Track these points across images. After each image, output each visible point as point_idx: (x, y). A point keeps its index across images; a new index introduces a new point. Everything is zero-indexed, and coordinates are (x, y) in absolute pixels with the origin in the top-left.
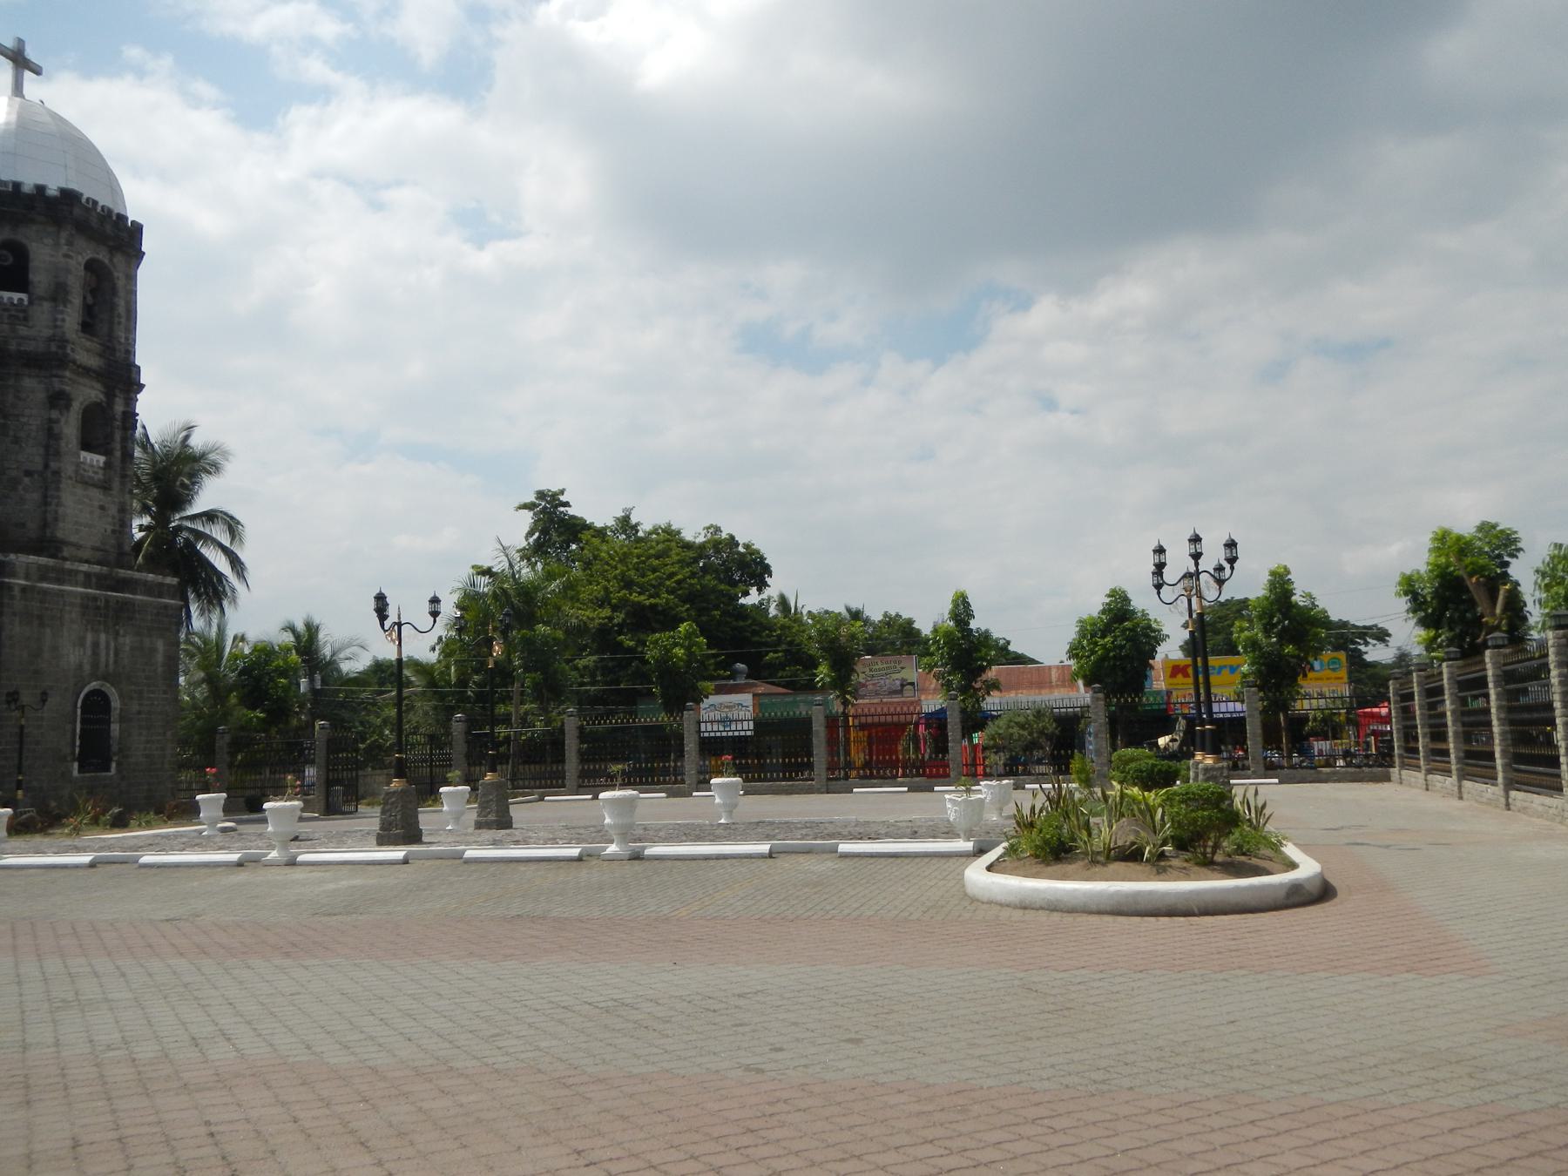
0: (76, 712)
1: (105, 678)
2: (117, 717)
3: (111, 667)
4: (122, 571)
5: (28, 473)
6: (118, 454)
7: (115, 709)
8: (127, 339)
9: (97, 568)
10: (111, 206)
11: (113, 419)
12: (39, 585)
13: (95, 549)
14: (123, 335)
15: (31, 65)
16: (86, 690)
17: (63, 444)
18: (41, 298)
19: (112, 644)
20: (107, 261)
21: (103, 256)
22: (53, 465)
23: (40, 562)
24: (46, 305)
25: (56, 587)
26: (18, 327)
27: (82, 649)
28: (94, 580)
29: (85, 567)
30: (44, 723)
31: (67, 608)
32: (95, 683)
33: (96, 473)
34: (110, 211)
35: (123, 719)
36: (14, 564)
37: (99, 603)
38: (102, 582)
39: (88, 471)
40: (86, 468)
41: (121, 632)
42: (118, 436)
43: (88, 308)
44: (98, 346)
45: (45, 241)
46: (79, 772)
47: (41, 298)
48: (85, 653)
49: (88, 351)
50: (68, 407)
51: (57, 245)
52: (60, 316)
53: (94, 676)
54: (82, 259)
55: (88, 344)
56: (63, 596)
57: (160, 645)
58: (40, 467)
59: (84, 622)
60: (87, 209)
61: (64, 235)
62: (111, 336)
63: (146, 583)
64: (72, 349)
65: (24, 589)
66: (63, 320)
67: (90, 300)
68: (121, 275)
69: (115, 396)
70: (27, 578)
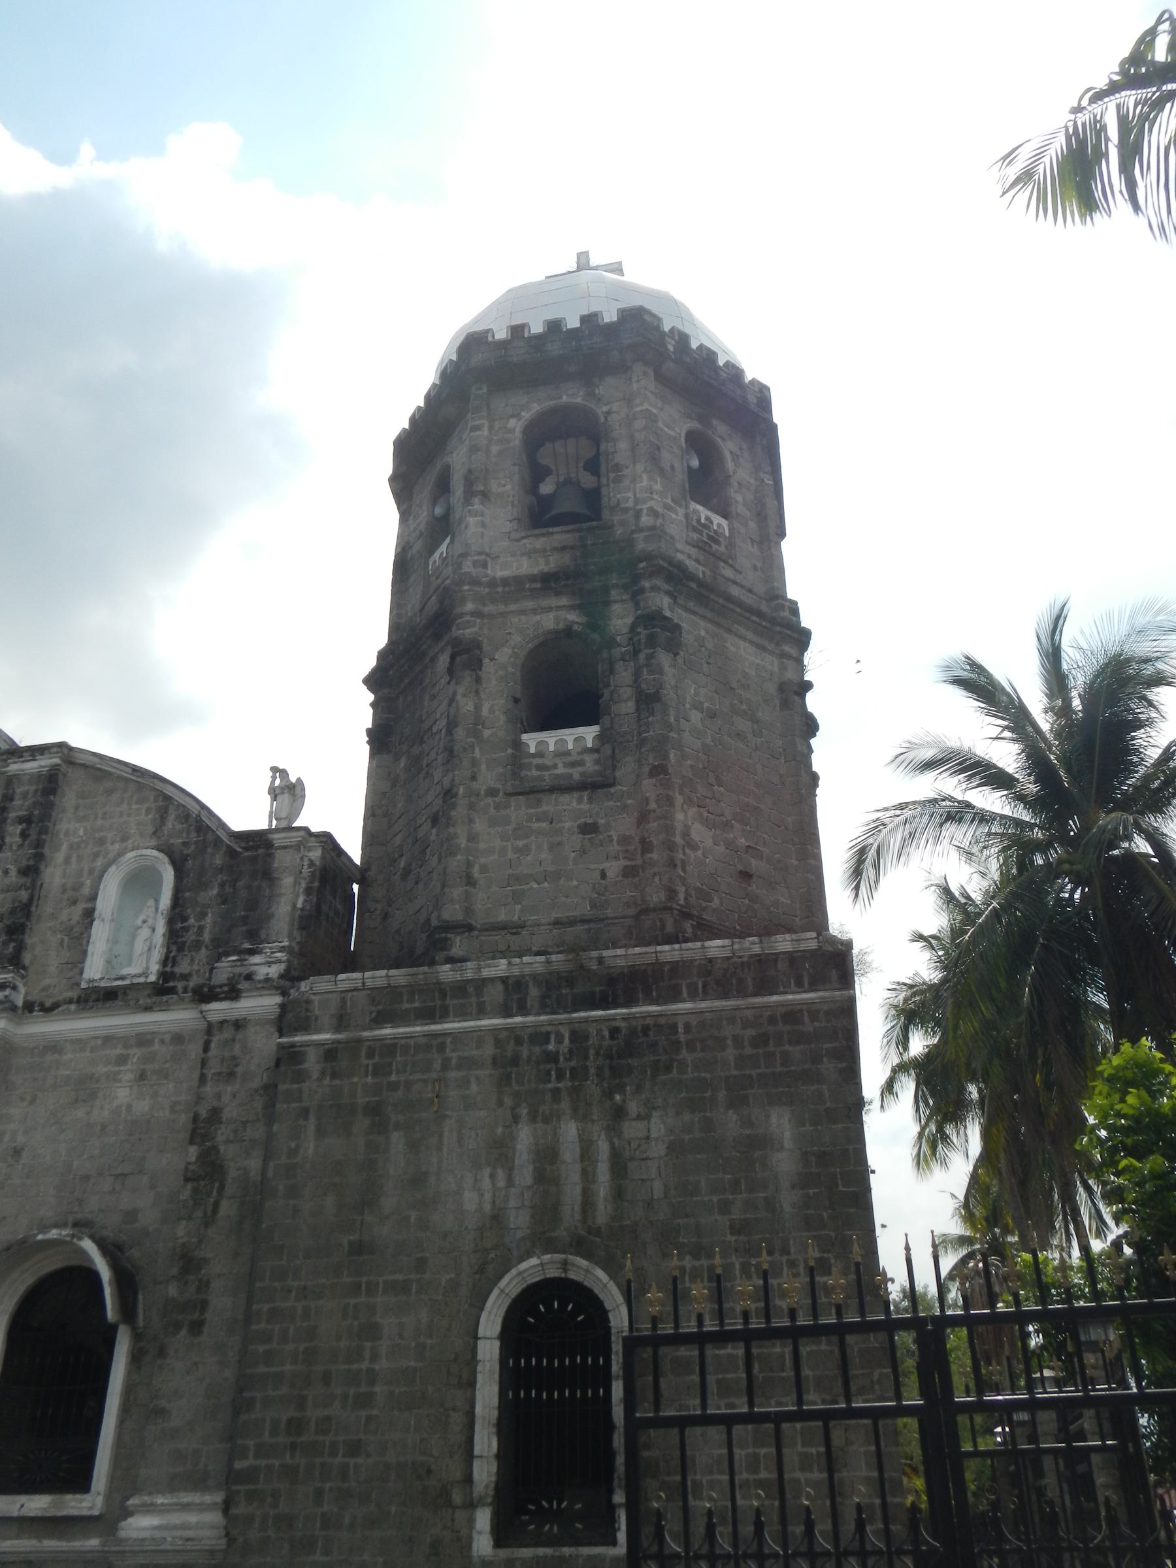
0: (472, 1361)
1: (580, 1246)
3: (603, 1213)
4: (620, 952)
11: (611, 643)
12: (366, 1034)
13: (572, 922)
16: (510, 1285)
19: (603, 1148)
23: (369, 984)
25: (418, 1029)
27: (501, 1174)
28: (534, 992)
29: (500, 967)
30: (377, 1389)
32: (534, 1261)
33: (573, 764)
36: (308, 1002)
41: (633, 1108)
42: (624, 675)
46: (498, 1543)
48: (510, 1183)
50: (475, 664)
53: (542, 1241)
54: (516, 426)
55: (539, 543)
56: (441, 1048)
59: (508, 1101)
64: (475, 564)
65: (330, 1053)
67: (588, 480)
68: (615, 407)
69: (607, 603)
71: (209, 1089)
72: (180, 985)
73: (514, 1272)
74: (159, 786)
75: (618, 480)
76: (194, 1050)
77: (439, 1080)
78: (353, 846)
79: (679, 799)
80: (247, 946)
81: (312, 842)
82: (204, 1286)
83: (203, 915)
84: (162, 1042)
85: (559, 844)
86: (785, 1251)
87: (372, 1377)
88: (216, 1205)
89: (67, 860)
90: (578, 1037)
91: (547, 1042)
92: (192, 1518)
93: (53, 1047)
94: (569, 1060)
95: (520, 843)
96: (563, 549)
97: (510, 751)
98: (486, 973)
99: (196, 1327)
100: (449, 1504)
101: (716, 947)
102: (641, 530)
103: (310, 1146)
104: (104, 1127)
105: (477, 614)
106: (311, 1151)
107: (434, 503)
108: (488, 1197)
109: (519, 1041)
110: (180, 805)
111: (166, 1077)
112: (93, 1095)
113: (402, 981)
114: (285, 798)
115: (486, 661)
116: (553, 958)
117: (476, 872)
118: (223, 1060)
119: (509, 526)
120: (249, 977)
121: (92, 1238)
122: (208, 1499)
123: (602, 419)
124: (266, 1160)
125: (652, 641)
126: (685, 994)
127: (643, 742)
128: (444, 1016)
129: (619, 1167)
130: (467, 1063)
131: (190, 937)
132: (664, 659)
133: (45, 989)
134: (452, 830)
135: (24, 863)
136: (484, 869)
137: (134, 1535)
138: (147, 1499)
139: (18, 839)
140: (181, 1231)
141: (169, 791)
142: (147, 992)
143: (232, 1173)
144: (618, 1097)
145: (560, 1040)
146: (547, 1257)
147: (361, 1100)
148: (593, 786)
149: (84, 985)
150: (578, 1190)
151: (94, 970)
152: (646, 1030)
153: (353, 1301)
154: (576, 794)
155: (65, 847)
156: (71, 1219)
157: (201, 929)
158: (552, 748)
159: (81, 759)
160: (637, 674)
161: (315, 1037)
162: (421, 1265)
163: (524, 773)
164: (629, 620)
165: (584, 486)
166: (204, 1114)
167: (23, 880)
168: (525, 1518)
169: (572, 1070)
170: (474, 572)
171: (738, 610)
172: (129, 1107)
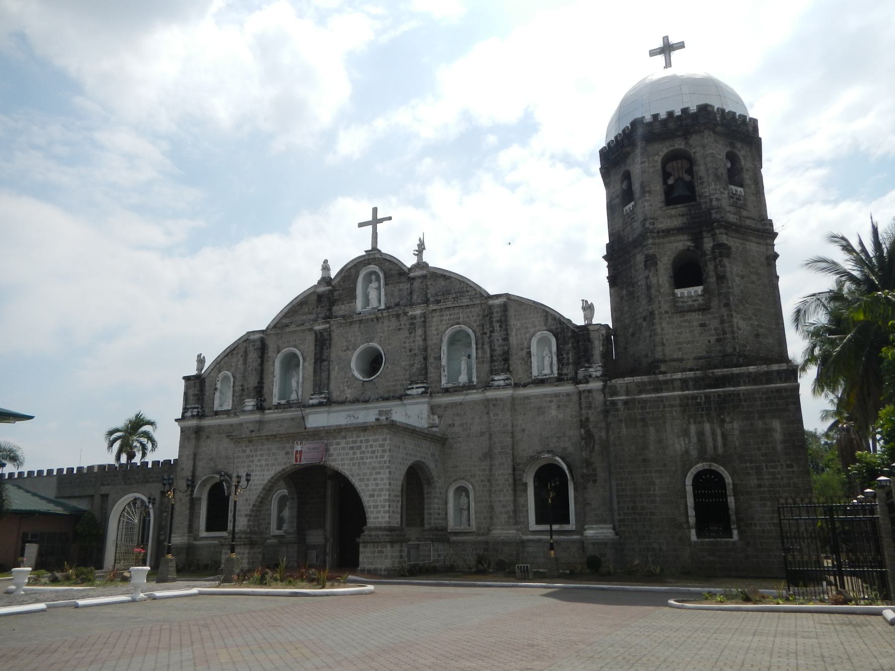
1: (714, 460)
2: (731, 490)
3: (720, 450)
4: (720, 370)
6: (713, 280)
7: (729, 484)
9: (691, 374)
11: (705, 254)
12: (637, 397)
13: (700, 358)
15: (674, 46)
16: (694, 471)
19: (719, 431)
20: (682, 147)
21: (679, 144)
23: (635, 381)
25: (654, 395)
26: (633, 224)
27: (686, 439)
28: (691, 383)
29: (679, 375)
31: (667, 409)
32: (700, 464)
33: (694, 301)
35: (736, 493)
36: (616, 386)
37: (698, 401)
38: (698, 383)
39: (688, 302)
41: (727, 419)
42: (711, 267)
44: (681, 209)
48: (690, 442)
49: (671, 217)
50: (655, 264)
53: (702, 457)
54: (659, 159)
55: (673, 212)
56: (662, 401)
57: (777, 424)
59: (686, 417)
63: (749, 375)
64: (650, 223)
65: (626, 403)
67: (687, 178)
68: (698, 149)
69: (702, 238)
70: (628, 393)
71: (584, 412)
72: (565, 377)
73: (694, 467)
74: (543, 308)
75: (702, 183)
76: (575, 398)
77: (662, 411)
78: (611, 326)
79: (734, 314)
80: (587, 365)
81: (602, 328)
82: (594, 470)
83: (568, 354)
84: (563, 396)
85: (693, 331)
86: (779, 461)
87: (655, 495)
88: (594, 447)
89: (516, 335)
90: (707, 397)
91: (697, 399)
92: (605, 531)
93: (528, 398)
94: (705, 405)
95: (679, 331)
96: (683, 215)
97: (672, 297)
98: (674, 377)
99: (595, 481)
101: (752, 369)
102: (714, 209)
103: (624, 431)
104: (550, 422)
105: (654, 244)
106: (625, 433)
107: (622, 182)
108: (683, 446)
109: (688, 399)
110: (552, 314)
111: (567, 407)
112: (544, 413)
113: (646, 380)
114: (588, 311)
115: (659, 262)
116: (697, 372)
117: (665, 341)
118: (586, 403)
119: (660, 205)
120: (590, 376)
121: (558, 456)
122: (608, 526)
123: (693, 156)
124: (607, 432)
125: (721, 255)
126: (742, 384)
127: (720, 294)
128: (661, 391)
129: (724, 437)
130: (672, 406)
131: (565, 361)
132: (726, 261)
133: (520, 379)
134: (655, 327)
135: (503, 337)
136: (667, 340)
137: (589, 535)
138: (591, 526)
140: (584, 454)
141: (547, 310)
142: (555, 379)
143: (597, 437)
144: (722, 416)
145: (701, 398)
146: (704, 463)
147: (639, 417)
148: (704, 309)
149: (533, 378)
150: (712, 444)
151: (535, 373)
152: (730, 395)
153: (645, 475)
154: (697, 313)
155: (514, 330)
156: (546, 450)
157: (568, 359)
158: (686, 295)
159: (514, 298)
160: (716, 267)
161: (620, 398)
162: (665, 465)
163: (677, 304)
164: (711, 245)
165: (686, 180)
166: (584, 419)
167: (504, 343)
168: (705, 531)
169: (706, 408)
170: (651, 227)
171: (750, 231)
172: (557, 416)
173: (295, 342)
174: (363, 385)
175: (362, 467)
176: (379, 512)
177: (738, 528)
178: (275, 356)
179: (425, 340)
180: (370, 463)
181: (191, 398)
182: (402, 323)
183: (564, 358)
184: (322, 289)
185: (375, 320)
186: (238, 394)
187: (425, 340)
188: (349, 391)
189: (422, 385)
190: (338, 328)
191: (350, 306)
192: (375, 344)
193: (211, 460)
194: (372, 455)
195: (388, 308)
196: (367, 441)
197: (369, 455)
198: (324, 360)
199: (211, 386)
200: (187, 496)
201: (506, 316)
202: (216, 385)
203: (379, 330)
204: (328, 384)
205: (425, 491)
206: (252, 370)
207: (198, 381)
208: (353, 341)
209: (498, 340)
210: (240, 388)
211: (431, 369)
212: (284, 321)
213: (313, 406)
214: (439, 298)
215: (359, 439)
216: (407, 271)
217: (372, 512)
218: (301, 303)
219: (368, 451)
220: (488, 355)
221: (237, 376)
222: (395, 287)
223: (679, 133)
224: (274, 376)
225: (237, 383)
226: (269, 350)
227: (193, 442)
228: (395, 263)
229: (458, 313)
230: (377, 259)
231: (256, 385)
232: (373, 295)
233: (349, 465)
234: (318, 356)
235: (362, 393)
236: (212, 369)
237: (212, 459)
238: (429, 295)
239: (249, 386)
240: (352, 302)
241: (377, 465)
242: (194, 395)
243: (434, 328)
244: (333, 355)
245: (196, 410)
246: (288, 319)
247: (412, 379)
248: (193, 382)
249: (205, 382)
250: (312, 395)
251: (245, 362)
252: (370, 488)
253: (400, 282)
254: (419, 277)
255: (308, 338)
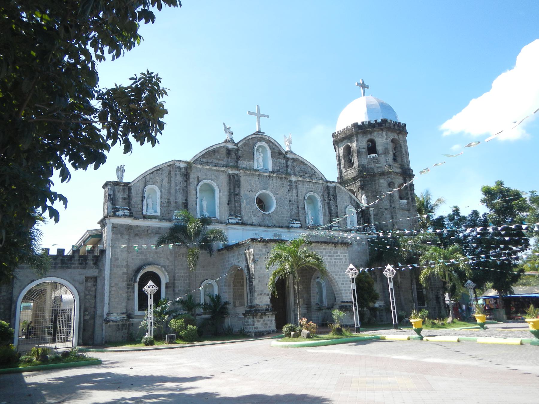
5: (386, 209)
6: (410, 199)
8: (407, 161)
10: (395, 120)
14: (405, 160)
15: (366, 86)
17: (394, 198)
18: (381, 154)
20: (397, 138)
21: (396, 137)
22: (393, 205)
24: (383, 156)
33: (405, 206)
34: (396, 122)
40: (402, 205)
43: (394, 154)
45: (379, 136)
47: (381, 154)
49: (397, 167)
51: (383, 136)
52: (387, 158)
54: (390, 139)
55: (396, 165)
58: (389, 207)
60: (390, 123)
61: (384, 133)
62: (402, 161)
66: (389, 159)
68: (402, 141)
69: (406, 180)
75: (404, 157)
83: (360, 219)
100: (411, 302)
139: (333, 199)
167: (336, 207)
173: (212, 177)
174: (263, 215)
175: (336, 267)
176: (347, 293)
177: (427, 302)
178: (196, 183)
179: (297, 196)
180: (340, 265)
181: (121, 200)
182: (284, 183)
183: (359, 221)
184: (230, 146)
185: (268, 177)
186: (165, 205)
187: (297, 196)
188: (255, 218)
189: (298, 222)
190: (244, 175)
191: (250, 163)
192: (268, 192)
193: (140, 253)
194: (340, 261)
195: (273, 172)
196: (337, 253)
197: (339, 261)
198: (237, 195)
199: (137, 194)
200: (123, 281)
201: (336, 193)
202: (143, 193)
203: (271, 184)
204: (240, 211)
205: (311, 284)
206: (180, 189)
207: (127, 188)
208: (254, 187)
209: (333, 205)
210: (167, 201)
211: (300, 215)
212: (201, 160)
213: (232, 224)
214: (301, 174)
215: (333, 251)
216: (284, 153)
217: (344, 293)
218: (214, 150)
219: (338, 258)
220: (327, 212)
221: (163, 191)
222: (276, 160)
223: (398, 132)
224: (197, 198)
225: (163, 197)
226: (190, 177)
227: (127, 237)
228: (276, 145)
229: (311, 186)
230: (265, 139)
231: (184, 201)
232: (261, 160)
233: (329, 265)
234: (232, 191)
235: (263, 221)
236: (138, 181)
237: (142, 253)
238: (296, 171)
239: (178, 201)
240: (251, 161)
241: (343, 267)
242: (124, 199)
243: (300, 191)
244: (242, 193)
245: (126, 211)
246: (204, 159)
247: (292, 218)
248: (121, 187)
249: (131, 189)
250: (229, 216)
251: (169, 182)
252: (341, 279)
253: (280, 158)
254: (291, 159)
255: (221, 177)
